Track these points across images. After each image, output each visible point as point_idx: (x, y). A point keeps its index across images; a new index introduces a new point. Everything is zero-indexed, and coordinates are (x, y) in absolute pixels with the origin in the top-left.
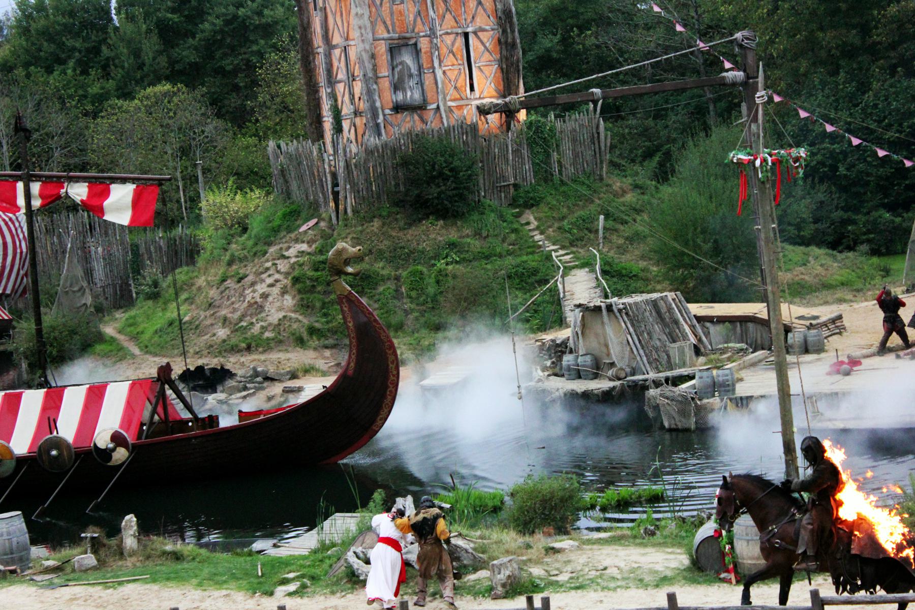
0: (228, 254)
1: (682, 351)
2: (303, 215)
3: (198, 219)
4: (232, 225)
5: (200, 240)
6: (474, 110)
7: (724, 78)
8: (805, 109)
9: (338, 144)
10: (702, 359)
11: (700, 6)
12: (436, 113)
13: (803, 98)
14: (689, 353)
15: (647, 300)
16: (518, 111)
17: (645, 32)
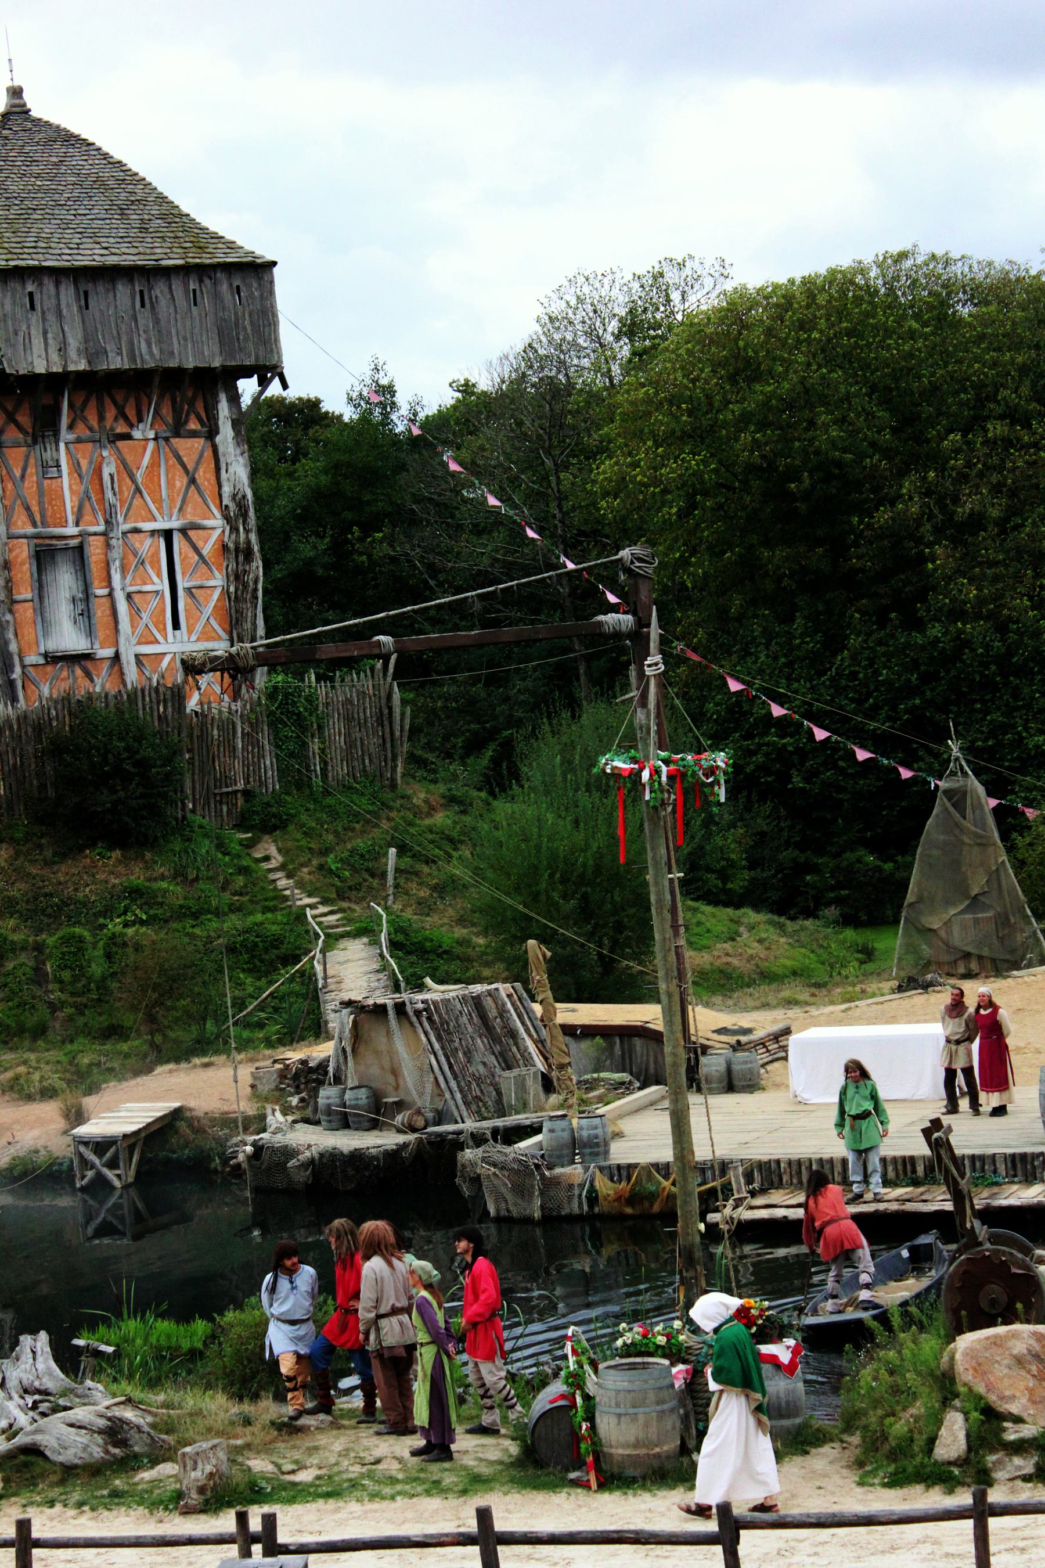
1: (521, 1085)
8: (737, 679)
10: (554, 1099)
11: (566, 498)
12: (112, 666)
13: (734, 658)
14: (534, 1088)
15: (464, 997)
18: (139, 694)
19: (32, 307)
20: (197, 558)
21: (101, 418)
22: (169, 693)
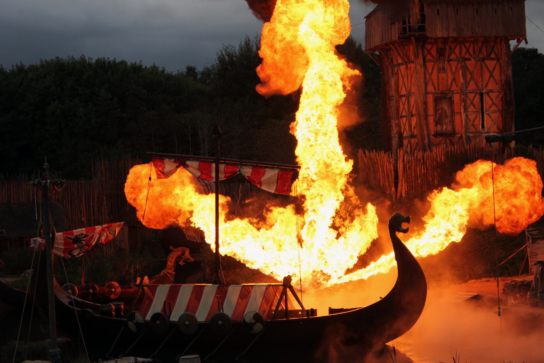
16: (511, 142)
18: (468, 150)
19: (438, 14)
20: (492, 103)
21: (461, 53)
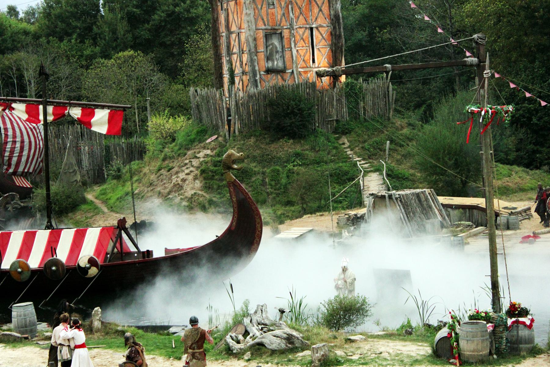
0: (163, 154)
2: (209, 133)
3: (145, 133)
4: (166, 137)
5: (147, 145)
6: (314, 74)
7: (465, 61)
9: (232, 91)
11: (453, 18)
13: (513, 76)
15: (413, 193)
16: (341, 76)
17: (420, 32)
18: (300, 85)
22: (310, 85)
